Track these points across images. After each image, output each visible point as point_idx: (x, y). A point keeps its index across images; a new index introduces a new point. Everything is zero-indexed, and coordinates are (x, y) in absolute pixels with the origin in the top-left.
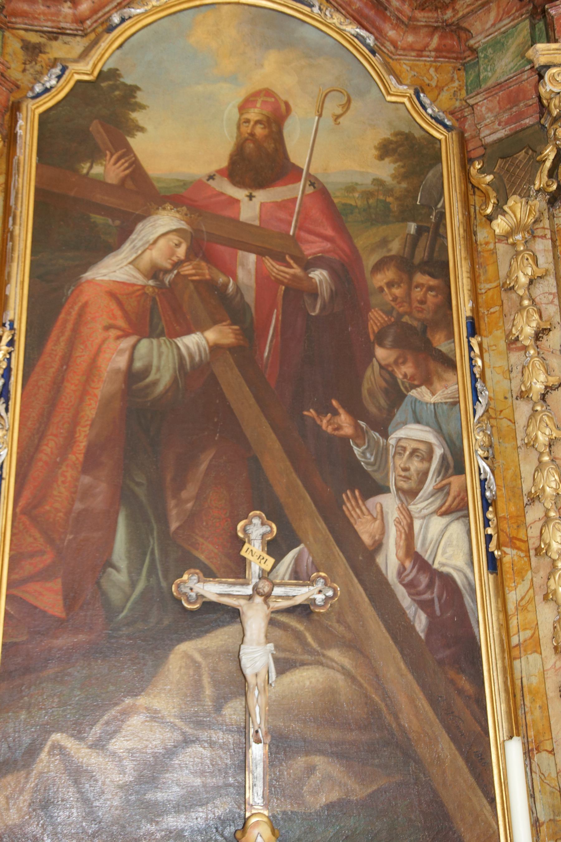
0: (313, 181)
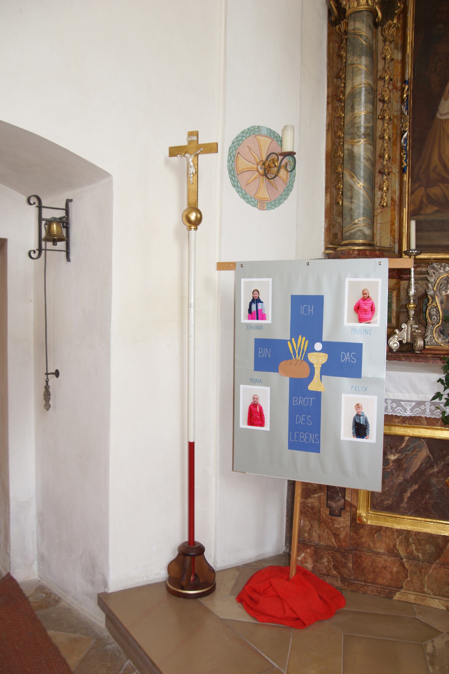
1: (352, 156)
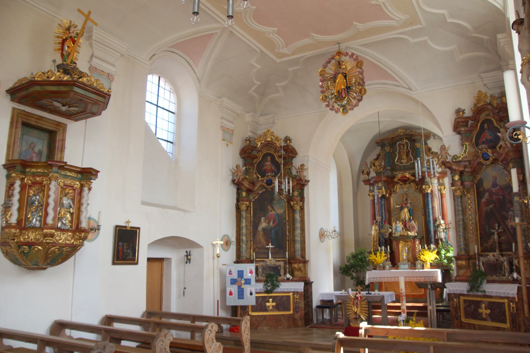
1: (242, 240)
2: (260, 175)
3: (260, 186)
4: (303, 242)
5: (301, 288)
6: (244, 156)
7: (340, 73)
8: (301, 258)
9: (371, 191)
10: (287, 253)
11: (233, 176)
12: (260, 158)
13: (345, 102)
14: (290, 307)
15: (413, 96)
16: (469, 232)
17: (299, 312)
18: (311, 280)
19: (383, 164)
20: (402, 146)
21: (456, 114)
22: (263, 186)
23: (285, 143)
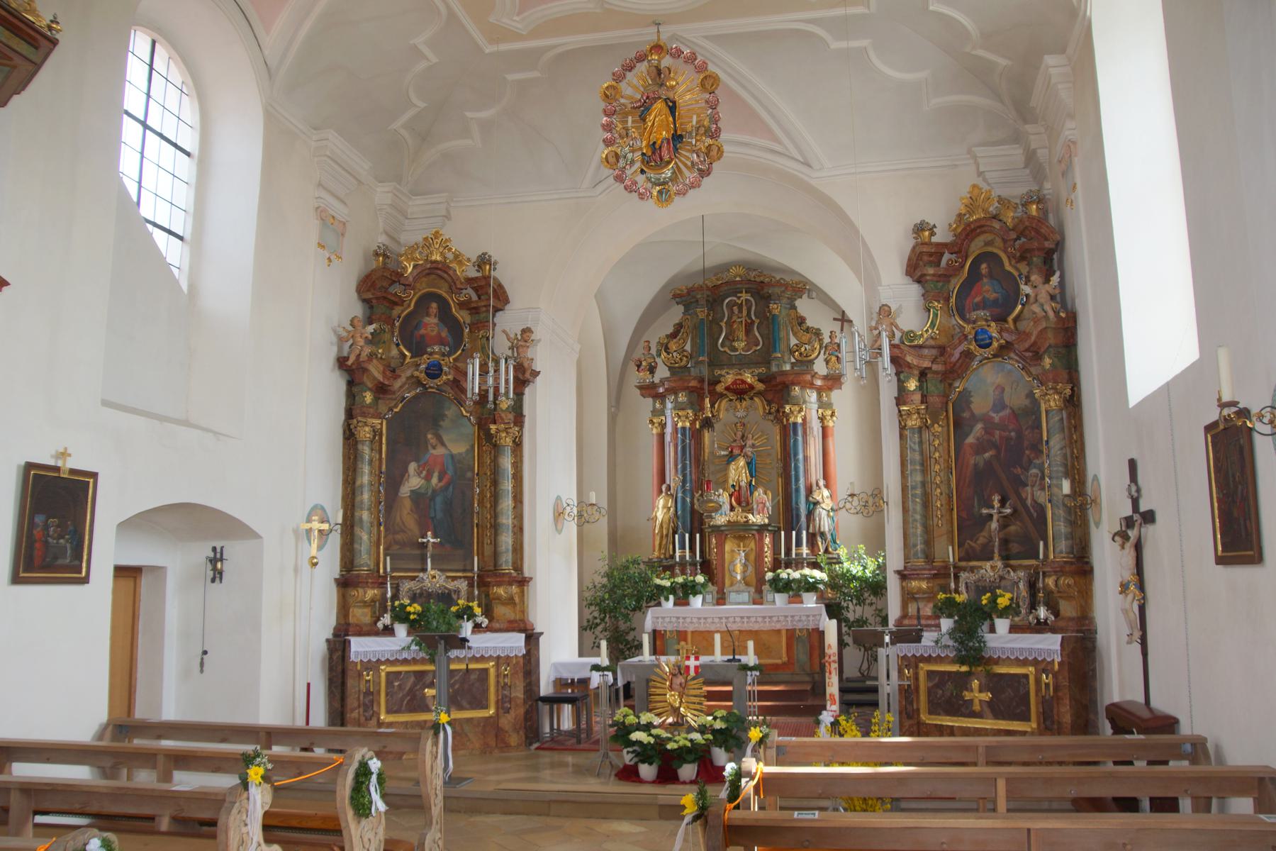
0: (1011, 408)
2: (409, 350)
3: (408, 378)
4: (519, 530)
5: (517, 645)
6: (369, 296)
7: (660, 98)
8: (512, 571)
9: (656, 413)
10: (476, 559)
11: (340, 349)
12: (409, 306)
13: (667, 173)
14: (487, 699)
15: (814, 183)
16: (934, 513)
17: (512, 712)
18: (538, 630)
19: (688, 347)
20: (735, 308)
21: (915, 235)
22: (414, 380)
23: (478, 271)
